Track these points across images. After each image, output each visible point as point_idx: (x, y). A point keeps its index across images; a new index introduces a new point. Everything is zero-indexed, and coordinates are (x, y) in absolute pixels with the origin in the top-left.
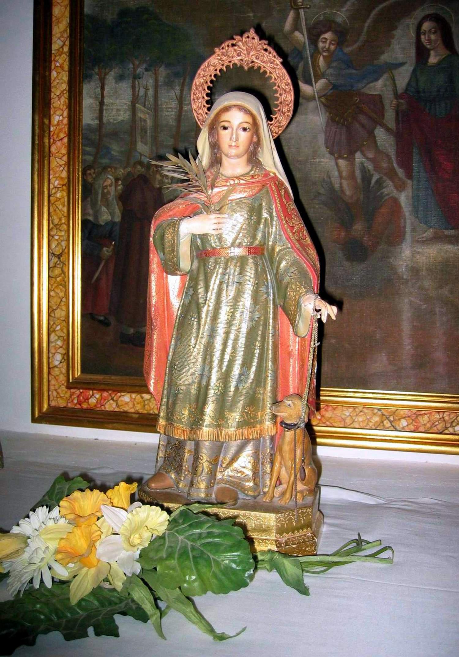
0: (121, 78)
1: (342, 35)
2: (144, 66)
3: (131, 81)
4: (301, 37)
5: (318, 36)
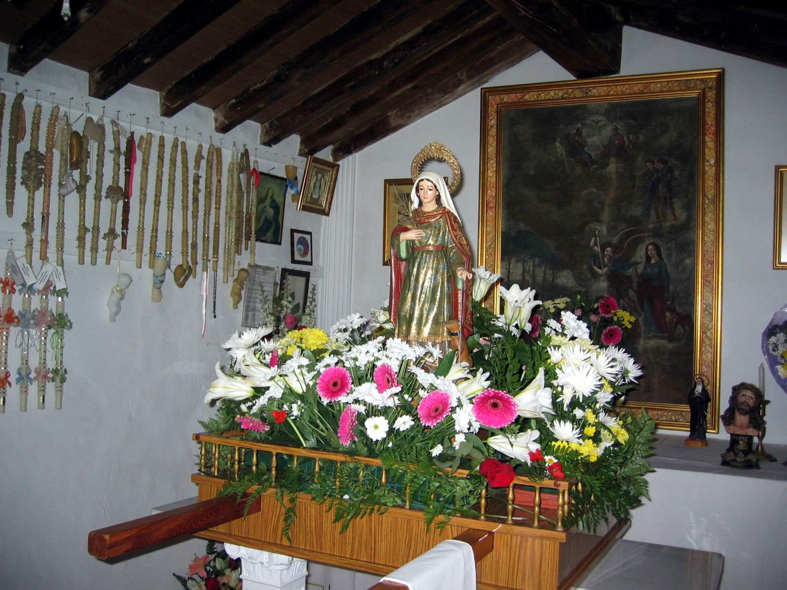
0: (517, 261)
1: (615, 249)
2: (528, 257)
3: (522, 264)
4: (597, 249)
5: (605, 249)
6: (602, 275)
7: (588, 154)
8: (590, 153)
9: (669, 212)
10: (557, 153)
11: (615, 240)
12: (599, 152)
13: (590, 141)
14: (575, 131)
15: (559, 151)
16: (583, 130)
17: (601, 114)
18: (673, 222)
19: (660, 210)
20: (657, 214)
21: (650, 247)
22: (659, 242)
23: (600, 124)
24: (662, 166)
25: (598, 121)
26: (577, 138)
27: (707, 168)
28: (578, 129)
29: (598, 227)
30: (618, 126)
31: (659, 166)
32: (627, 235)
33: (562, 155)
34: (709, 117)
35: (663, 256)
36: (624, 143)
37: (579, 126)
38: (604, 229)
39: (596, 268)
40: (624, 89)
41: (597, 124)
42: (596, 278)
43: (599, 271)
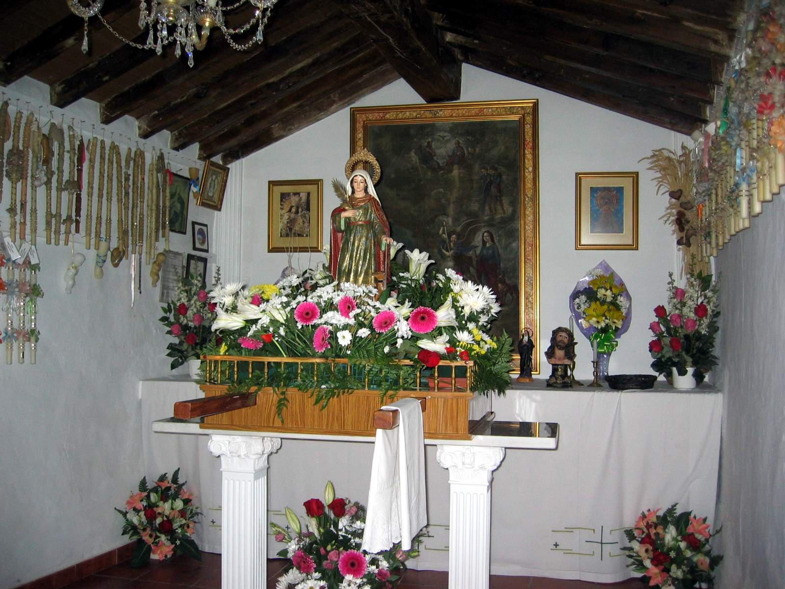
1: (459, 236)
4: (445, 236)
5: (451, 236)
6: (449, 257)
8: (438, 161)
9: (499, 207)
10: (412, 161)
11: (459, 229)
13: (438, 152)
14: (426, 144)
15: (414, 159)
16: (433, 144)
17: (445, 131)
18: (503, 215)
19: (492, 206)
20: (490, 208)
21: (485, 234)
22: (492, 230)
23: (445, 138)
24: (493, 172)
26: (428, 149)
27: (526, 174)
28: (429, 143)
29: (445, 219)
30: (461, 141)
31: (491, 172)
32: (469, 224)
33: (416, 163)
34: (528, 135)
35: (496, 241)
36: (464, 154)
37: (430, 140)
38: (450, 220)
39: (444, 251)
42: (444, 259)
43: (447, 254)
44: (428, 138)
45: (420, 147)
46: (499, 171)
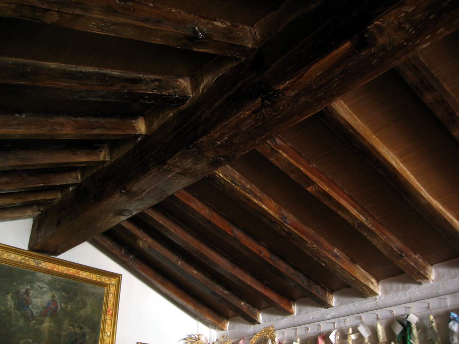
7: (31, 310)
8: (33, 310)
10: (7, 304)
12: (39, 311)
13: (34, 301)
14: (24, 290)
15: (9, 303)
16: (31, 292)
17: (45, 283)
23: (43, 289)
24: (79, 331)
25: (43, 288)
26: (25, 296)
28: (27, 290)
30: (56, 295)
31: (78, 330)
34: (110, 303)
36: (57, 308)
37: (29, 287)
40: (63, 269)
41: (41, 289)
44: (27, 285)
45: (18, 292)
46: (84, 330)
